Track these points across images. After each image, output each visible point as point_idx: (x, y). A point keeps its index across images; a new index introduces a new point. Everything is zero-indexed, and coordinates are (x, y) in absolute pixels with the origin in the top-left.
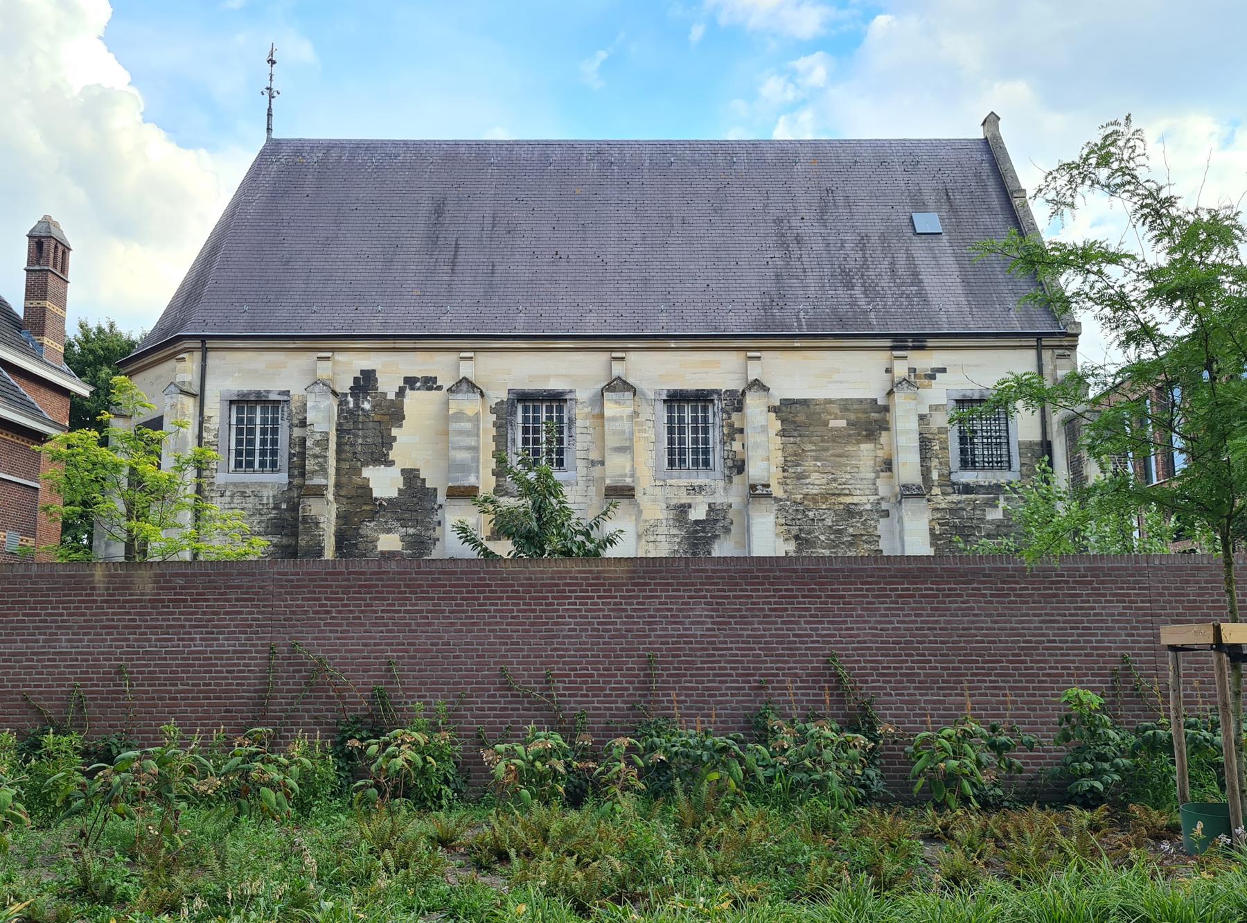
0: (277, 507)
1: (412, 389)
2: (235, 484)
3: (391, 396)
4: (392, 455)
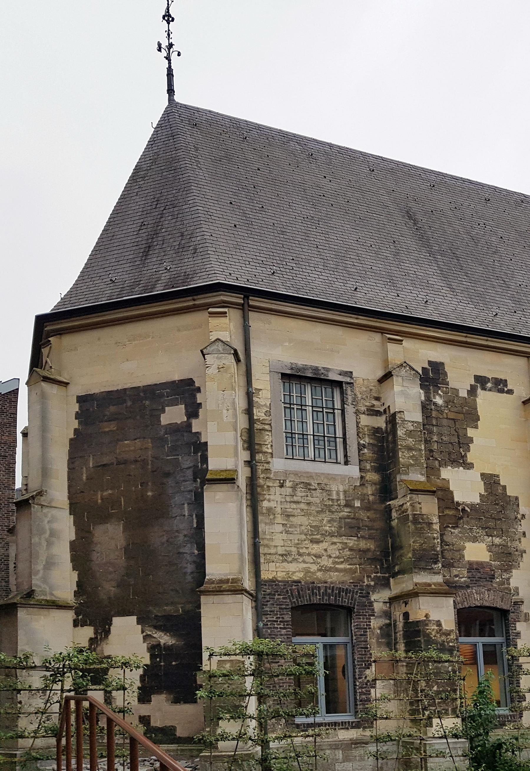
0: (348, 505)
1: (484, 388)
2: (296, 474)
3: (463, 394)
4: (470, 458)
